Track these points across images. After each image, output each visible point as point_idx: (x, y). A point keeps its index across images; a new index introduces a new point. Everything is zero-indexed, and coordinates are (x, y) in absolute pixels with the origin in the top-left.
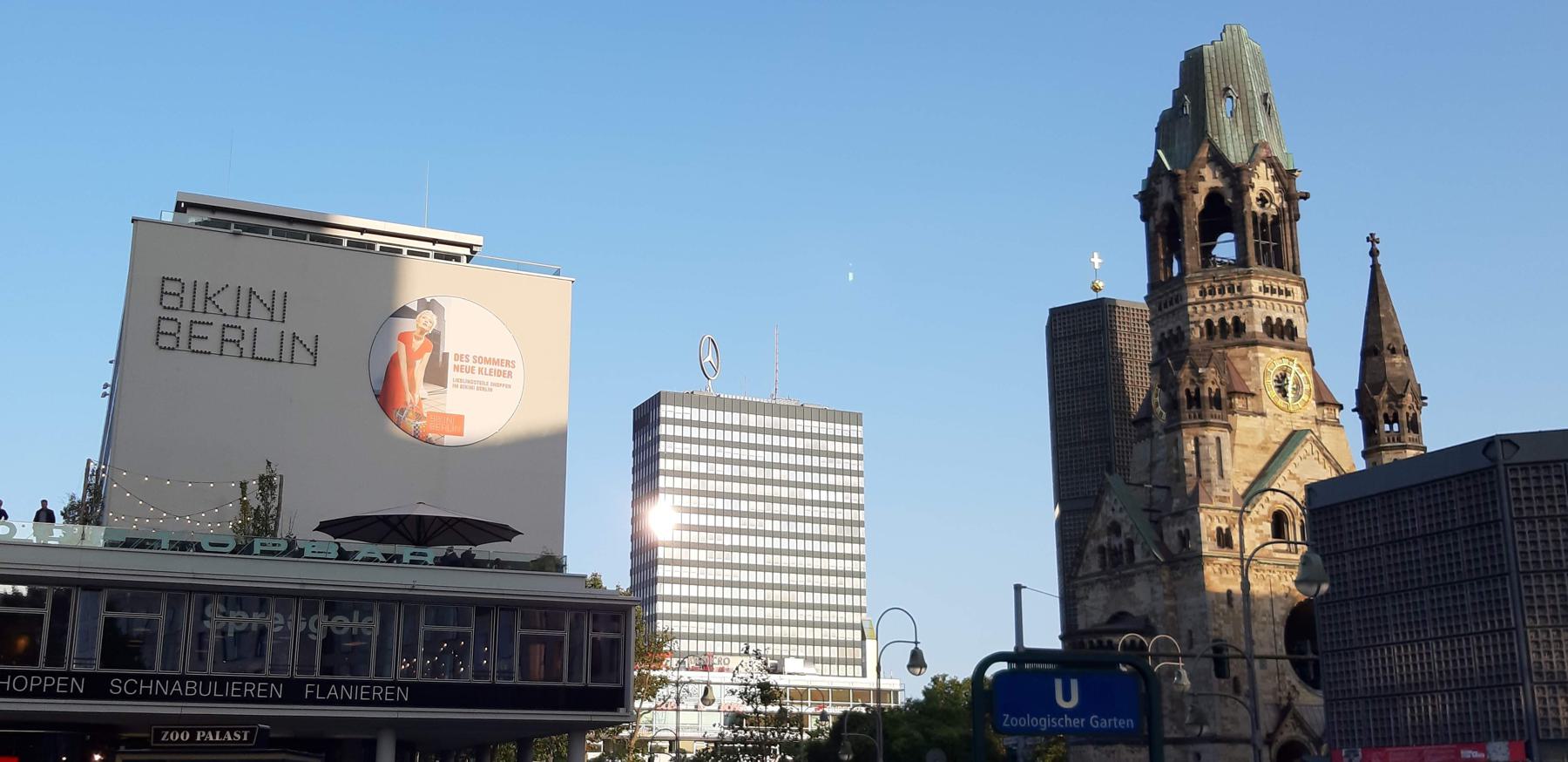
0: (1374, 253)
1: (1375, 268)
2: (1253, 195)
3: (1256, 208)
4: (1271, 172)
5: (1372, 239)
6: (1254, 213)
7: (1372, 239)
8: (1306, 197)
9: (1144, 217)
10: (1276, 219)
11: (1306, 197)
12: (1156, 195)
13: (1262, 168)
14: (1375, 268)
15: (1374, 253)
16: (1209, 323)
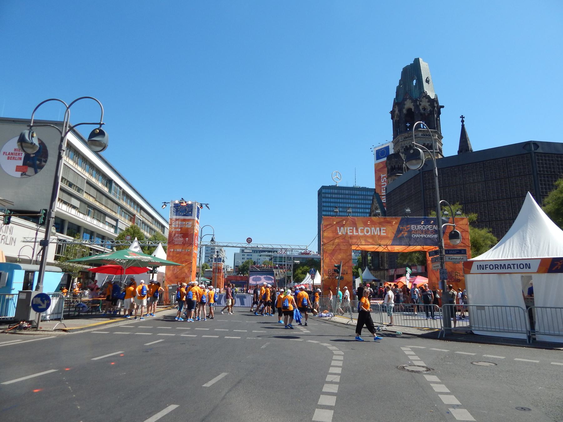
0: (463, 121)
1: (463, 126)
2: (421, 107)
3: (422, 111)
4: (427, 100)
5: (462, 117)
6: (421, 114)
7: (462, 117)
8: (443, 107)
9: (392, 118)
10: (429, 115)
11: (443, 107)
12: (395, 111)
13: (424, 100)
14: (463, 126)
15: (463, 121)
16: (406, 147)
